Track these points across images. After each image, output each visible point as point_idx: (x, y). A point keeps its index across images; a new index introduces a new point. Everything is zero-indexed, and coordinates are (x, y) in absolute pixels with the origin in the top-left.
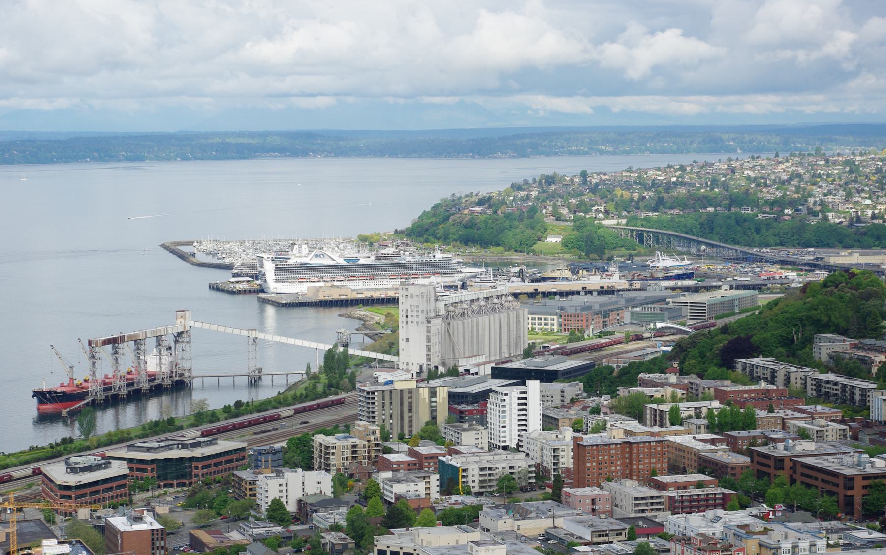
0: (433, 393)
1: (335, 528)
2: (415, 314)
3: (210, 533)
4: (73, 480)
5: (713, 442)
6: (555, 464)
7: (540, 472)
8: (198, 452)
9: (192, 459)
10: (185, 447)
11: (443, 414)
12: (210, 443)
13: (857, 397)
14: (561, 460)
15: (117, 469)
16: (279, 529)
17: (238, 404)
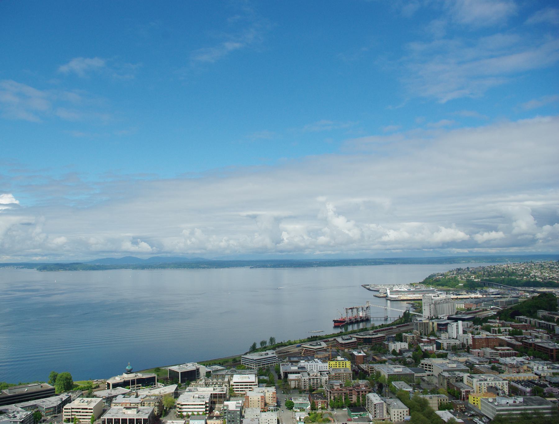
0: (433, 323)
1: (409, 357)
2: (426, 303)
3: (378, 357)
4: (343, 342)
5: (511, 338)
6: (467, 343)
7: (463, 345)
8: (373, 336)
9: (372, 338)
10: (370, 335)
11: (436, 329)
12: (376, 334)
13: (551, 327)
14: (469, 342)
15: (354, 340)
16: (395, 357)
17: (382, 325)
